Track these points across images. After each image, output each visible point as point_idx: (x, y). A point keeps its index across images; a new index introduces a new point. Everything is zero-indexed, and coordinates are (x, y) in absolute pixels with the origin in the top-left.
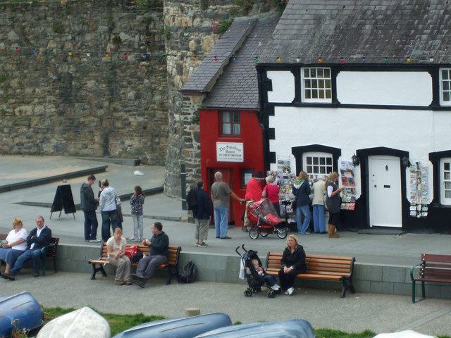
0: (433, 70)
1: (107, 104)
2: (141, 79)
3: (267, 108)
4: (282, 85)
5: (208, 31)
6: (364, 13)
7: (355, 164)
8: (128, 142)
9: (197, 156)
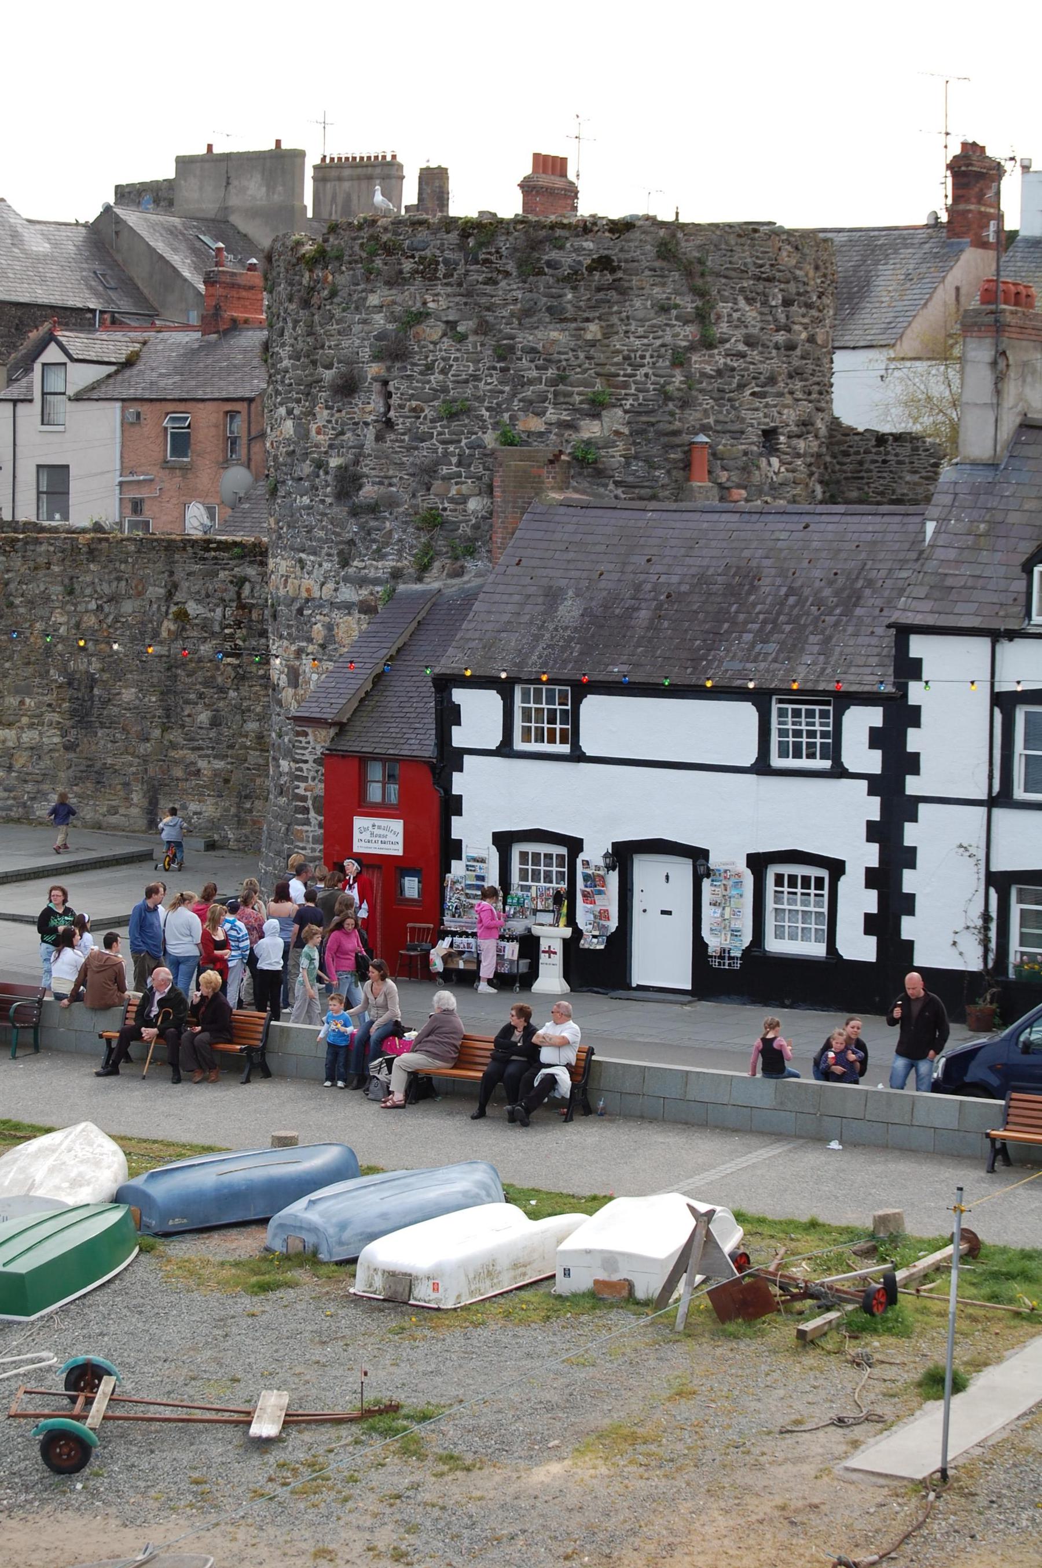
0: (761, 699)
1: (157, 733)
2: (222, 690)
3: (450, 759)
4: (479, 716)
5: (347, 607)
6: (638, 588)
7: (610, 868)
8: (193, 807)
9: (316, 841)
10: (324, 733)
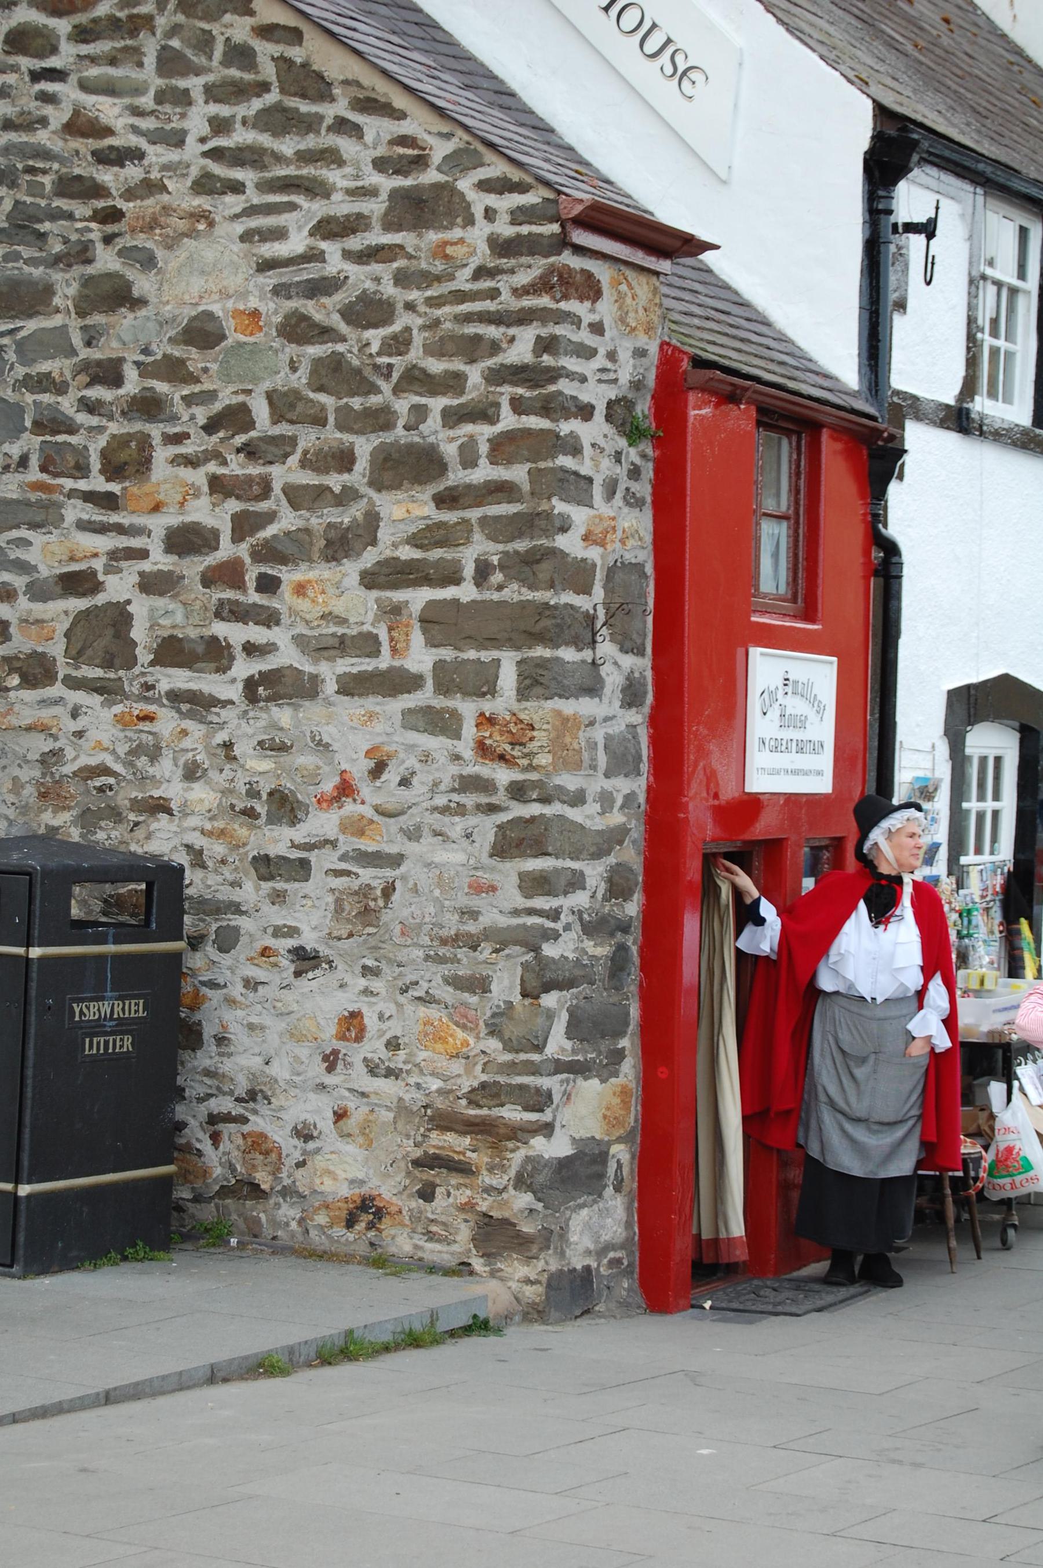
9: (621, 762)
10: (642, 287)
